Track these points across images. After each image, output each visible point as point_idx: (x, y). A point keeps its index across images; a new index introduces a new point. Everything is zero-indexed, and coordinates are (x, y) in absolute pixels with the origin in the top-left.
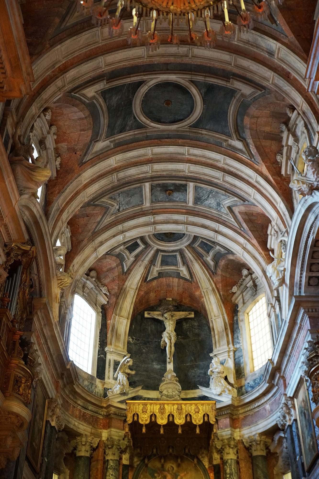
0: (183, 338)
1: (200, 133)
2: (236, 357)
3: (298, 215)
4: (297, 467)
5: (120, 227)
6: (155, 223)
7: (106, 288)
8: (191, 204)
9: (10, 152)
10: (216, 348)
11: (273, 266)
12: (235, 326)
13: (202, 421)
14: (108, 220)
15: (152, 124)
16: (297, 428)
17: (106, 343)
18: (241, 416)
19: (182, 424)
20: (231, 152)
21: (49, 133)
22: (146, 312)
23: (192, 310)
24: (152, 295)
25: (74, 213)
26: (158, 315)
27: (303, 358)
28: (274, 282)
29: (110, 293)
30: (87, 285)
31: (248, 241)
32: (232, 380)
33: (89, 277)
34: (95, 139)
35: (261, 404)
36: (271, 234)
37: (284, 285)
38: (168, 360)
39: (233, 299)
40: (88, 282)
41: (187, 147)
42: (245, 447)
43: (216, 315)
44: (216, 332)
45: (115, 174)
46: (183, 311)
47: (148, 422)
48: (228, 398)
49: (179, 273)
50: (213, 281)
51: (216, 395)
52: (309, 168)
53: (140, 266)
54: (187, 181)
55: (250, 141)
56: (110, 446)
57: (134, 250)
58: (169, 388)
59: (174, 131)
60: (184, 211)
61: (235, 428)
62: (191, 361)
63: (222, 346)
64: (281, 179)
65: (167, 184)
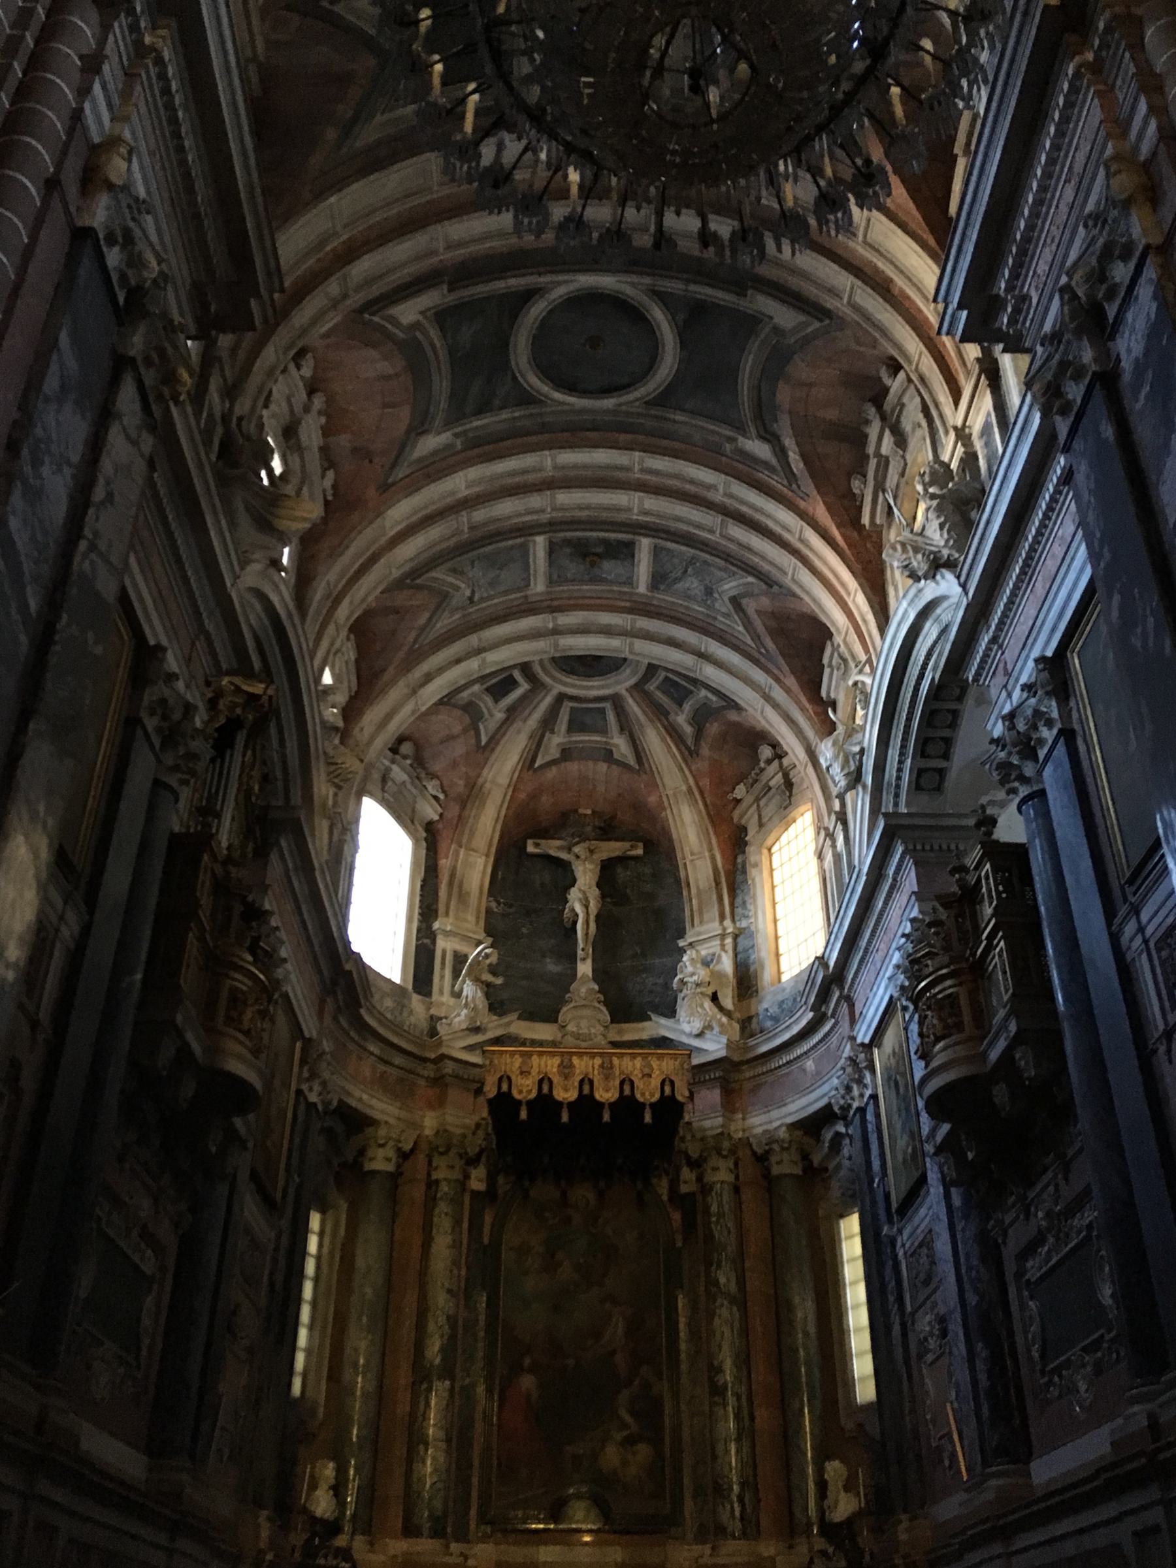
0: (615, 904)
1: (669, 420)
2: (740, 948)
3: (899, 624)
4: (874, 1202)
5: (473, 640)
6: (556, 632)
7: (435, 782)
8: (642, 589)
9: (219, 457)
10: (693, 925)
11: (834, 744)
12: (739, 878)
13: (657, 1096)
14: (446, 622)
15: (557, 395)
16: (877, 1115)
17: (436, 911)
18: (748, 1086)
19: (612, 1100)
20: (741, 466)
21: (307, 409)
22: (530, 842)
23: (638, 839)
24: (546, 800)
25: (364, 606)
26: (560, 848)
27: (896, 958)
28: (837, 779)
29: (446, 796)
30: (393, 775)
31: (777, 680)
32: (728, 1002)
33: (397, 757)
34: (419, 428)
35: (795, 1059)
36: (830, 666)
37: (860, 789)
38: (580, 953)
39: (736, 815)
40: (395, 768)
41: (637, 454)
42: (754, 1153)
43: (696, 851)
44: (694, 891)
45: (464, 513)
46: (617, 840)
47: (533, 1095)
48: (719, 1042)
49: (611, 752)
50: (691, 771)
51: (690, 1035)
52: (931, 515)
53: (519, 732)
54: (634, 534)
55: (789, 442)
56: (441, 1150)
57: (506, 693)
58: (582, 1017)
59: (607, 412)
60: (628, 604)
61: (733, 1111)
62: (635, 956)
63: (708, 922)
64: (860, 533)
65: (587, 539)
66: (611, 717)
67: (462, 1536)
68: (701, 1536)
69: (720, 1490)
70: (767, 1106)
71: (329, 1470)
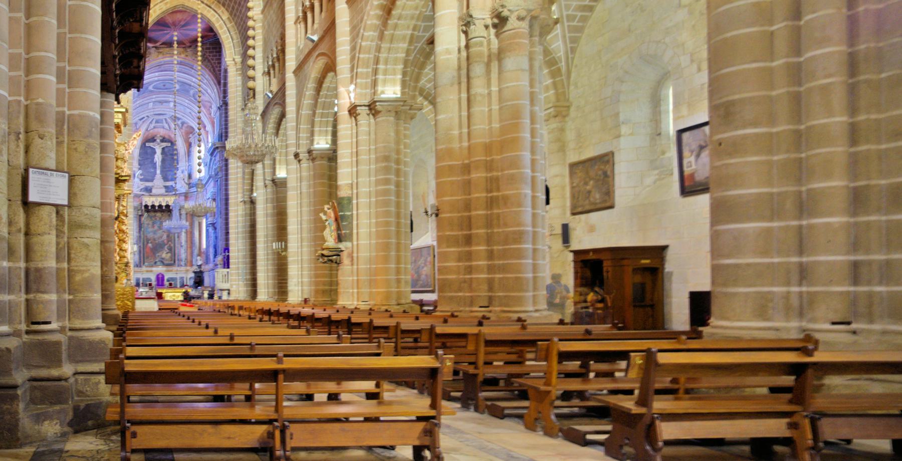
32: (186, 181)
39: (190, 140)
66: (164, 121)
67: (140, 266)
68: (178, 266)
69: (181, 260)
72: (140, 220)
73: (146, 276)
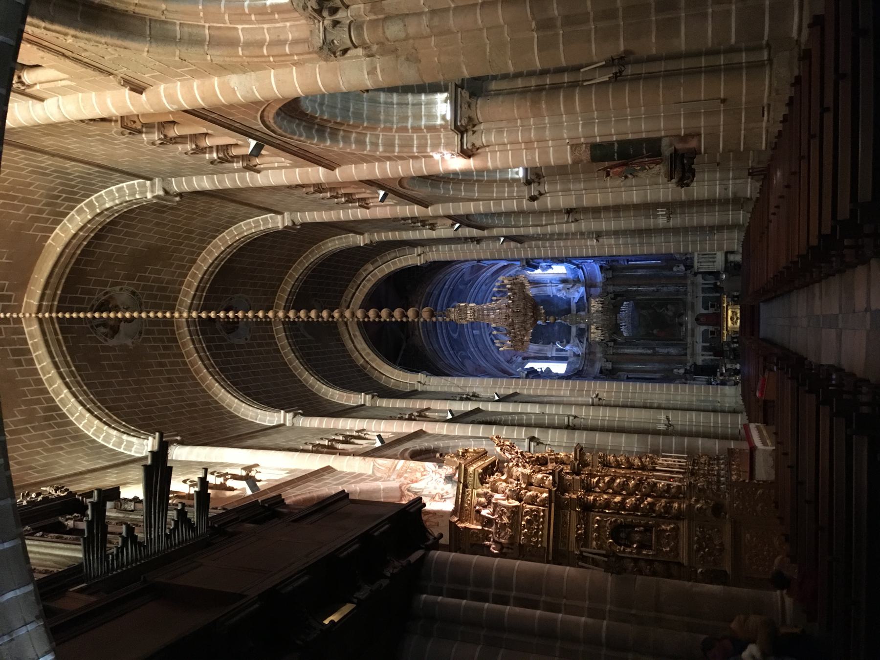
68: (686, 295)
69: (678, 291)
70: (596, 278)
71: (675, 370)
72: (621, 344)
73: (699, 338)
